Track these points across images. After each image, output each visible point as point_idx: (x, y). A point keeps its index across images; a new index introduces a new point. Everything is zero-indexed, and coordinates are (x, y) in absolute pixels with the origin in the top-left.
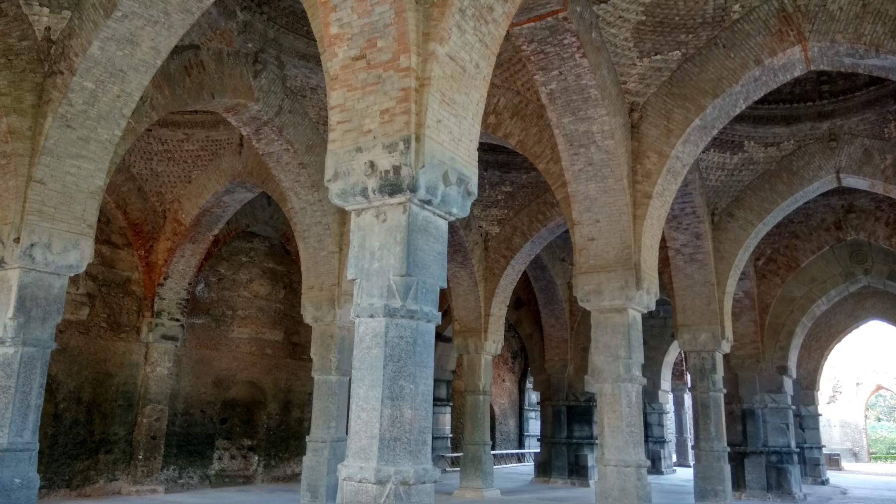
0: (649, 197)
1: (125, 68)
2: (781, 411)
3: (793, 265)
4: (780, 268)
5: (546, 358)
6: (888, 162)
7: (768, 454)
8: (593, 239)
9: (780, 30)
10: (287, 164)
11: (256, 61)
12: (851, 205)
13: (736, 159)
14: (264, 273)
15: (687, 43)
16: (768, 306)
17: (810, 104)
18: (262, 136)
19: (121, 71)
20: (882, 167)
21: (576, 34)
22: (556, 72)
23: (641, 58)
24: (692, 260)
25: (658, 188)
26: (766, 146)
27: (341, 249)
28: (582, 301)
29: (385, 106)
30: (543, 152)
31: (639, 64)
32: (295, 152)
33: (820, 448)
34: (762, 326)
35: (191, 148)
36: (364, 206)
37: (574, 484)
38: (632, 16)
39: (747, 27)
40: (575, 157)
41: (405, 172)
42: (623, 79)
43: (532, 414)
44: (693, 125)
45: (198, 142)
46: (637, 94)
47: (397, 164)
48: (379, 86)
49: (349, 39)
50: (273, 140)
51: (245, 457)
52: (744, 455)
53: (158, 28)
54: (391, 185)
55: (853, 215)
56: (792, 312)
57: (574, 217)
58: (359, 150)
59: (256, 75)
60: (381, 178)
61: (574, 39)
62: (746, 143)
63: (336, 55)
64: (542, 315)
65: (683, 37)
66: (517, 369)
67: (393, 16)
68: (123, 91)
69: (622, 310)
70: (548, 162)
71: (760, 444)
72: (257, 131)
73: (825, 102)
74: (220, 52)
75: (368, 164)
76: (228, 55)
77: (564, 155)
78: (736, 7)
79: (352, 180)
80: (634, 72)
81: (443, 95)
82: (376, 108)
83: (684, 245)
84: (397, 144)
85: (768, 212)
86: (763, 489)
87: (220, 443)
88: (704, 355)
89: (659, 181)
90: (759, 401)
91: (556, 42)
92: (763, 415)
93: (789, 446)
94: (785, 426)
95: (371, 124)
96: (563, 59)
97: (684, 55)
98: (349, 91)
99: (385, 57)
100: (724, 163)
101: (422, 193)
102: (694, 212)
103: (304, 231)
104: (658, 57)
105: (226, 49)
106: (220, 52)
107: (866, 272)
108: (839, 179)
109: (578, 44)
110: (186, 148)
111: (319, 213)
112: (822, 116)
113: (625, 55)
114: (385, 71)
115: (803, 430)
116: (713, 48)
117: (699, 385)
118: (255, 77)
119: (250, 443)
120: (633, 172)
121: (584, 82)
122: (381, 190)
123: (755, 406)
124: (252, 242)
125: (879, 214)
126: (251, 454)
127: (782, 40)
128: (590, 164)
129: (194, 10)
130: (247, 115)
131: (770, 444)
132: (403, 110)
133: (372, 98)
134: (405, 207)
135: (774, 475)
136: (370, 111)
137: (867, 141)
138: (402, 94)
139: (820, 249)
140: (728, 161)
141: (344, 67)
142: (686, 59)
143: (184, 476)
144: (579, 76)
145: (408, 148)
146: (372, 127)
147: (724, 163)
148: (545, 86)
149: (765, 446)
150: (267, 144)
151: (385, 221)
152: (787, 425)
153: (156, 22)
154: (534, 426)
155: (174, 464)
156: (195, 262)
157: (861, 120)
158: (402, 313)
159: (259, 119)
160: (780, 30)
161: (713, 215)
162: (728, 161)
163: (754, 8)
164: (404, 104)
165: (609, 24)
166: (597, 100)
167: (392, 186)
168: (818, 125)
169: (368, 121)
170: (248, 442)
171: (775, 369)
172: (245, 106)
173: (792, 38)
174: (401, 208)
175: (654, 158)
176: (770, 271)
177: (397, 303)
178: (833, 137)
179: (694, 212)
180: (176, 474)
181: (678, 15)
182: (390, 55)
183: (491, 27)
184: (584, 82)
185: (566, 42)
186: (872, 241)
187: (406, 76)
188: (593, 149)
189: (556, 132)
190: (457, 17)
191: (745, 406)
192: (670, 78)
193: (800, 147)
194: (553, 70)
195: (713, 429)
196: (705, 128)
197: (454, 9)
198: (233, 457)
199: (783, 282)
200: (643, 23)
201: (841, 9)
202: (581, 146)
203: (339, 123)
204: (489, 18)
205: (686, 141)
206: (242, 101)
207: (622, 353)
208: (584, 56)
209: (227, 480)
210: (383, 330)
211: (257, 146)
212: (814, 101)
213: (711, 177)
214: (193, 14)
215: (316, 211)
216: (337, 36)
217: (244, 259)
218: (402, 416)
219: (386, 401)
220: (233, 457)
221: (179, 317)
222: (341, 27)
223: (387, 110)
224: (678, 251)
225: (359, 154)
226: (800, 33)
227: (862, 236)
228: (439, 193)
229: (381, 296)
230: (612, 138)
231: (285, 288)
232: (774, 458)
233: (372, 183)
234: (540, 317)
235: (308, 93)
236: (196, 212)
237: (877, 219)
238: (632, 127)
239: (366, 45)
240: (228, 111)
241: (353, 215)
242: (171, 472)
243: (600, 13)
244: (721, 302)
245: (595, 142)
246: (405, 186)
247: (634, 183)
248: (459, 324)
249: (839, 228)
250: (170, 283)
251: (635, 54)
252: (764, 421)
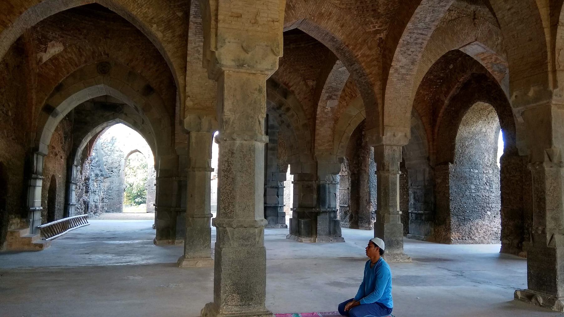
3: (354, 95)
5: (177, 141)
7: (330, 212)
28: (556, 95)
52: (318, 214)
56: (349, 124)
66: (66, 147)
71: (327, 207)
83: (402, 67)
86: (325, 235)
92: (329, 188)
115: (278, 196)
117: (390, 169)
123: (328, 182)
131: (331, 206)
135: (332, 224)
137: (490, 25)
168: (469, 6)
171: (337, 160)
191: (321, 182)
224: (396, 70)
248: (192, 100)
252: (329, 192)
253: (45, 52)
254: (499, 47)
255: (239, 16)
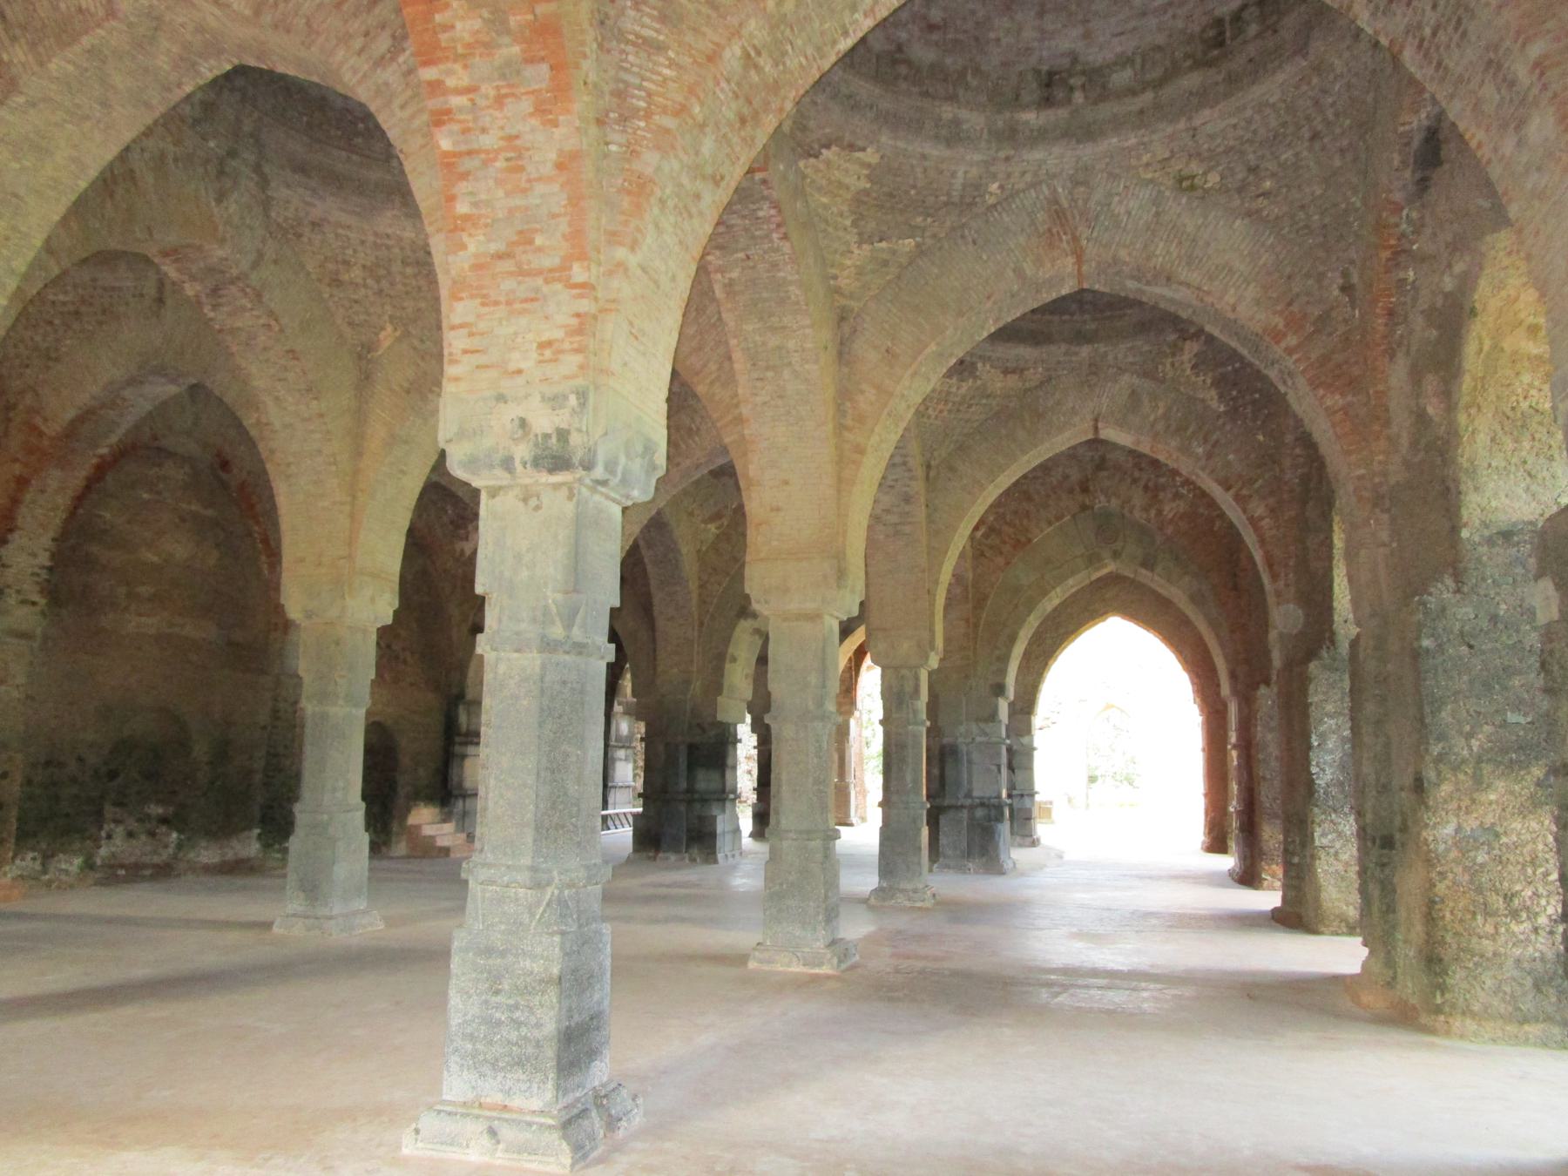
0: (861, 451)
1: (22, 192)
2: (991, 747)
3: (1023, 539)
4: (1005, 542)
5: (659, 669)
6: (1161, 411)
7: (972, 808)
8: (778, 509)
9: (1050, 230)
10: (265, 349)
11: (221, 173)
12: (1103, 459)
13: (965, 386)
14: (183, 520)
15: (924, 230)
16: (985, 598)
17: (1066, 317)
18: (223, 300)
19: (16, 196)
20: (1152, 418)
21: (776, 206)
22: (741, 255)
23: (860, 244)
24: (897, 533)
25: (875, 439)
26: (1006, 372)
27: (354, 497)
29: (545, 337)
30: (705, 366)
31: (856, 252)
32: (282, 331)
33: (1032, 795)
34: (976, 626)
35: (61, 297)
36: (504, 483)
37: (693, 860)
38: (850, 180)
39: (1007, 219)
40: (759, 384)
41: (575, 439)
42: (834, 271)
43: (621, 753)
44: (928, 350)
45: (75, 286)
46: (851, 296)
47: (564, 426)
48: (536, 304)
49: (486, 226)
50: (243, 309)
51: (152, 834)
53: (88, 124)
54: (554, 457)
55: (1105, 473)
56: (1016, 606)
57: (751, 474)
58: (501, 398)
59: (221, 197)
60: (536, 445)
61: (773, 212)
62: (980, 365)
63: (463, 247)
64: (656, 601)
65: (919, 219)
67: (564, 202)
68: (14, 229)
69: (815, 617)
70: (712, 383)
71: (961, 795)
72: (215, 291)
73: (1087, 317)
74: (162, 156)
75: (517, 422)
76: (176, 160)
77: (742, 379)
78: (994, 187)
79: (488, 442)
80: (849, 262)
81: (631, 324)
82: (530, 336)
83: (888, 511)
84: (565, 398)
85: (1002, 469)
87: (109, 810)
88: (905, 672)
89: (877, 429)
90: (964, 733)
91: (746, 212)
93: (999, 796)
94: (994, 768)
95: (525, 360)
96: (753, 237)
97: (918, 245)
98: (483, 304)
99: (548, 262)
100: (948, 393)
101: (599, 472)
102: (905, 463)
103: (289, 465)
104: (884, 245)
105: (171, 148)
106: (162, 156)
107: (1116, 555)
108: (1096, 429)
109: (778, 219)
110: (51, 297)
111: (318, 436)
112: (1081, 337)
113: (839, 238)
114: (547, 282)
116: (960, 241)
118: (219, 200)
119: (160, 811)
120: (840, 411)
121: (782, 274)
122: (537, 462)
123: (960, 740)
124: (160, 465)
125: (1137, 474)
126: (164, 829)
127: (1051, 246)
128: (781, 397)
129: (154, 102)
130: (202, 265)
131: (976, 793)
132: (575, 346)
133: (523, 321)
134: (571, 489)
136: (519, 340)
137: (1136, 380)
138: (574, 322)
139: (1058, 518)
140: (954, 390)
141: (478, 267)
142: (920, 251)
143: (52, 869)
144: (774, 265)
145: (583, 405)
146: (523, 365)
147: (948, 393)
148: (722, 272)
149: (969, 795)
150: (230, 314)
151: (537, 508)
152: (999, 767)
153: (87, 118)
154: (628, 772)
155: (33, 849)
156: (63, 501)
157: (1131, 349)
158: (567, 648)
159: (222, 272)
160: (1050, 230)
161: (929, 467)
162: (954, 390)
163: (1018, 192)
164: (578, 338)
165: (820, 189)
166: (797, 303)
167: (555, 459)
168: (1074, 349)
169: (516, 355)
170: (156, 810)
172: (200, 248)
173: (1064, 245)
174: (564, 492)
175: (871, 393)
176: (991, 547)
177: (557, 631)
178: (1094, 368)
179: (905, 463)
180: (37, 866)
181: (914, 187)
182: (557, 261)
183: (696, 222)
184: (782, 274)
185: (761, 214)
186: (1126, 511)
187: (582, 296)
188: (786, 374)
189: (733, 342)
190: (656, 211)
191: (946, 741)
192: (899, 277)
193: (1050, 379)
194: (737, 251)
195: (909, 778)
196: (941, 355)
197: (653, 200)
198: (130, 835)
199: (1008, 563)
200: (866, 192)
201: (1129, 213)
202: (768, 368)
203: (465, 352)
204: (694, 210)
205: (915, 374)
206: (197, 242)
207: (813, 679)
208: (785, 237)
209: (122, 872)
210: (537, 670)
211: (212, 315)
212: (1072, 314)
213: (930, 411)
214: (148, 105)
215: (312, 432)
216: (466, 218)
217: (146, 496)
218: (565, 794)
219: (543, 774)
220: (130, 835)
221: (36, 598)
222: (475, 204)
223: (549, 344)
225: (502, 405)
226: (1075, 239)
227: (1115, 503)
228: (620, 469)
229: (534, 620)
230: (816, 361)
231: (217, 546)
232: (980, 813)
233: (522, 452)
234: (651, 604)
235: (307, 231)
236: (71, 414)
237: (1135, 481)
238: (842, 343)
239: (515, 238)
240: (166, 254)
241: (483, 496)
242: (29, 862)
243: (809, 171)
244: (931, 593)
245: (790, 364)
246: (576, 460)
247: (841, 428)
249: (1085, 490)
250: (17, 539)
251: (852, 238)
252: (970, 762)
253: (467, 539)
254: (1160, 426)
255: (302, 560)
